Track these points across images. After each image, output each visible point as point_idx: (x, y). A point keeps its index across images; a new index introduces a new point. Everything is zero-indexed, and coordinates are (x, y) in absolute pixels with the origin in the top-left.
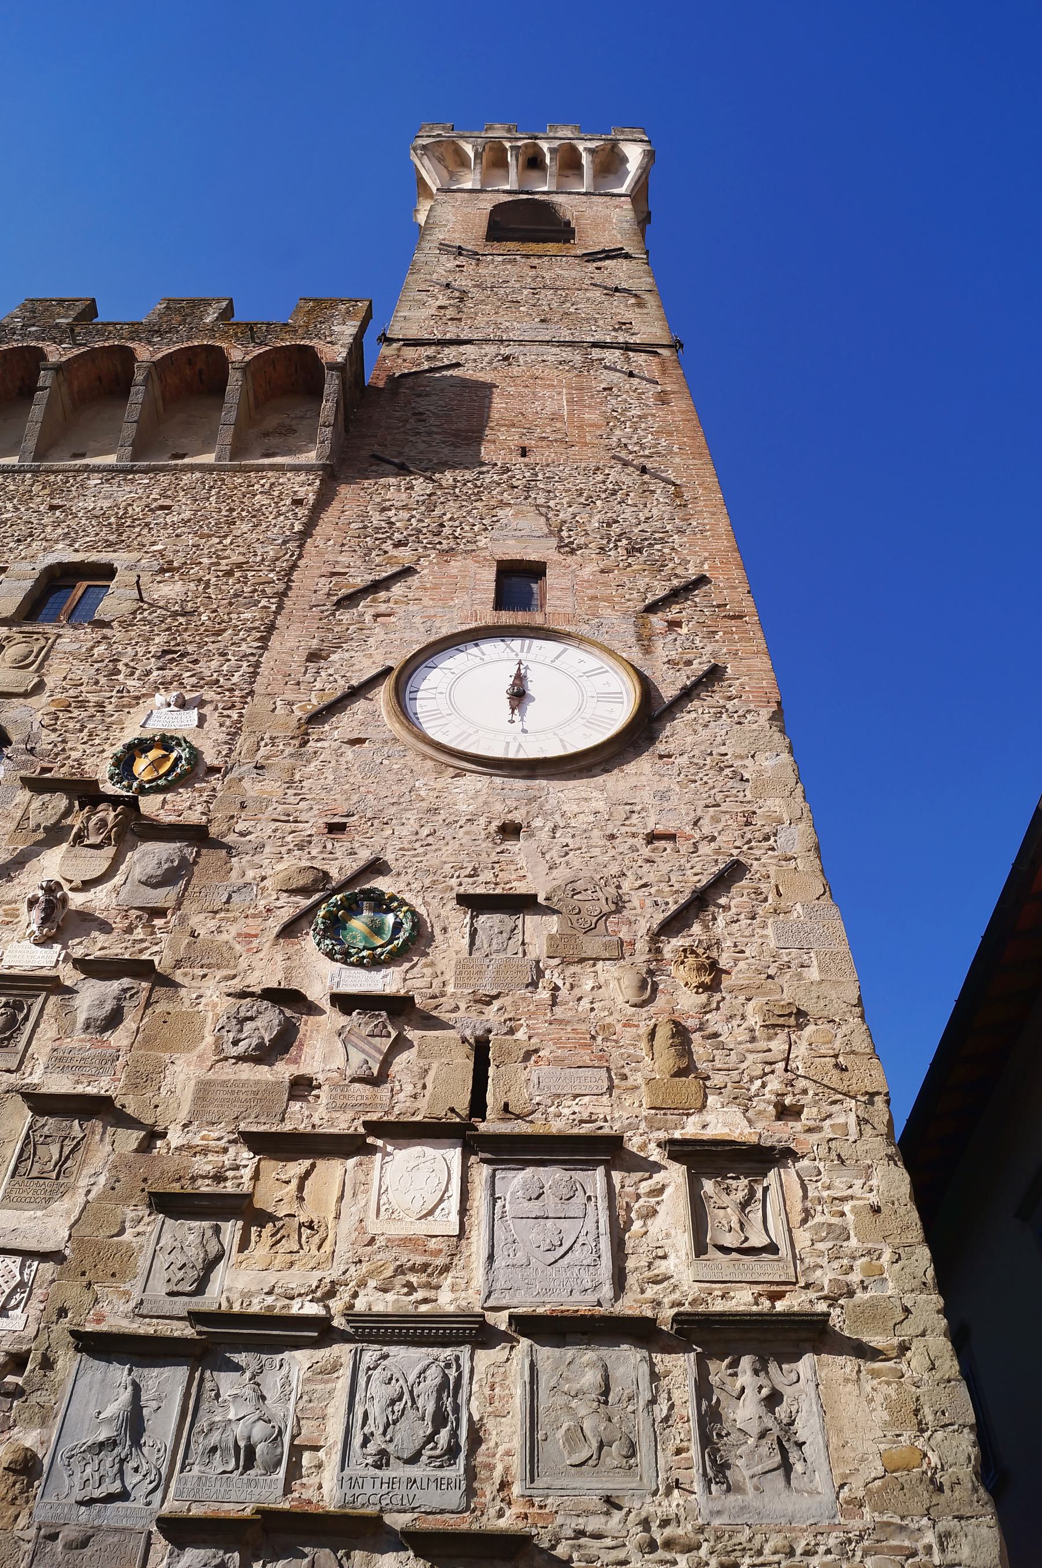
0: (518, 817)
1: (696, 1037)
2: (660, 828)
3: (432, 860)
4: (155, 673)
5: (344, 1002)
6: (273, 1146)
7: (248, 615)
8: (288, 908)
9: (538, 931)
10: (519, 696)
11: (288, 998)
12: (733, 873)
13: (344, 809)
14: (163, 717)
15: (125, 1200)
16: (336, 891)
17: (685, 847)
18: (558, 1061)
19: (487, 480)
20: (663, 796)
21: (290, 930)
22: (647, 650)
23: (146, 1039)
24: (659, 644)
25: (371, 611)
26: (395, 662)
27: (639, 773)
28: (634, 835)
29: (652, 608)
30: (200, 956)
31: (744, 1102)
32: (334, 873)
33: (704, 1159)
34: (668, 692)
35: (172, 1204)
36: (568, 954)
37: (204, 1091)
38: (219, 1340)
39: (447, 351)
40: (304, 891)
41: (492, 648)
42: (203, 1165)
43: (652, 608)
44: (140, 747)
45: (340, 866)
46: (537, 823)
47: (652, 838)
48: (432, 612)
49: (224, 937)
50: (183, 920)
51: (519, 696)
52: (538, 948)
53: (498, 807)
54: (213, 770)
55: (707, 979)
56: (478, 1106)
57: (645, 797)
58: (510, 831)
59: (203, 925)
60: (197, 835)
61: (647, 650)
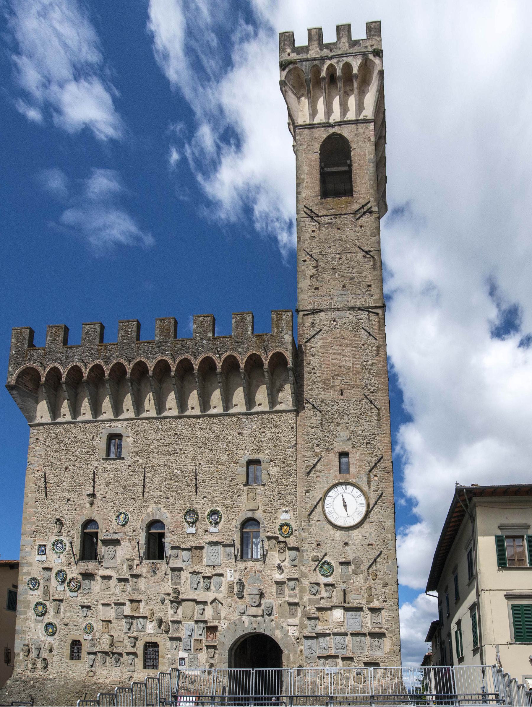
0: (347, 541)
1: (373, 589)
2: (370, 543)
3: (334, 553)
4: (279, 501)
5: (325, 585)
6: (320, 609)
7: (291, 480)
8: (314, 564)
9: (351, 568)
10: (345, 506)
11: (318, 584)
12: (381, 552)
13: (320, 540)
14: (284, 517)
15: (304, 617)
16: (320, 561)
17: (374, 546)
18: (355, 594)
19: (334, 410)
20: (370, 534)
21: (315, 570)
22: (369, 488)
23: (301, 592)
24: (372, 485)
25: (315, 476)
26: (321, 495)
27: (366, 525)
28: (365, 545)
29: (370, 471)
30: (303, 575)
31: (378, 600)
32: (320, 556)
33: (373, 610)
34: (372, 502)
35: (309, 618)
36: (355, 573)
37: (310, 599)
38: (319, 635)
39: (317, 317)
40: (316, 561)
41: (340, 489)
42: (312, 611)
43: (370, 471)
44: (282, 526)
45: (320, 556)
46: (350, 542)
47: (369, 545)
48: (327, 475)
49: (306, 571)
50: (299, 567)
51: (345, 506)
52: (351, 573)
53: (344, 538)
54: (296, 530)
55: (375, 578)
56: (345, 602)
57: (368, 535)
58: (346, 544)
59: (303, 568)
60: (297, 549)
61: (369, 488)
